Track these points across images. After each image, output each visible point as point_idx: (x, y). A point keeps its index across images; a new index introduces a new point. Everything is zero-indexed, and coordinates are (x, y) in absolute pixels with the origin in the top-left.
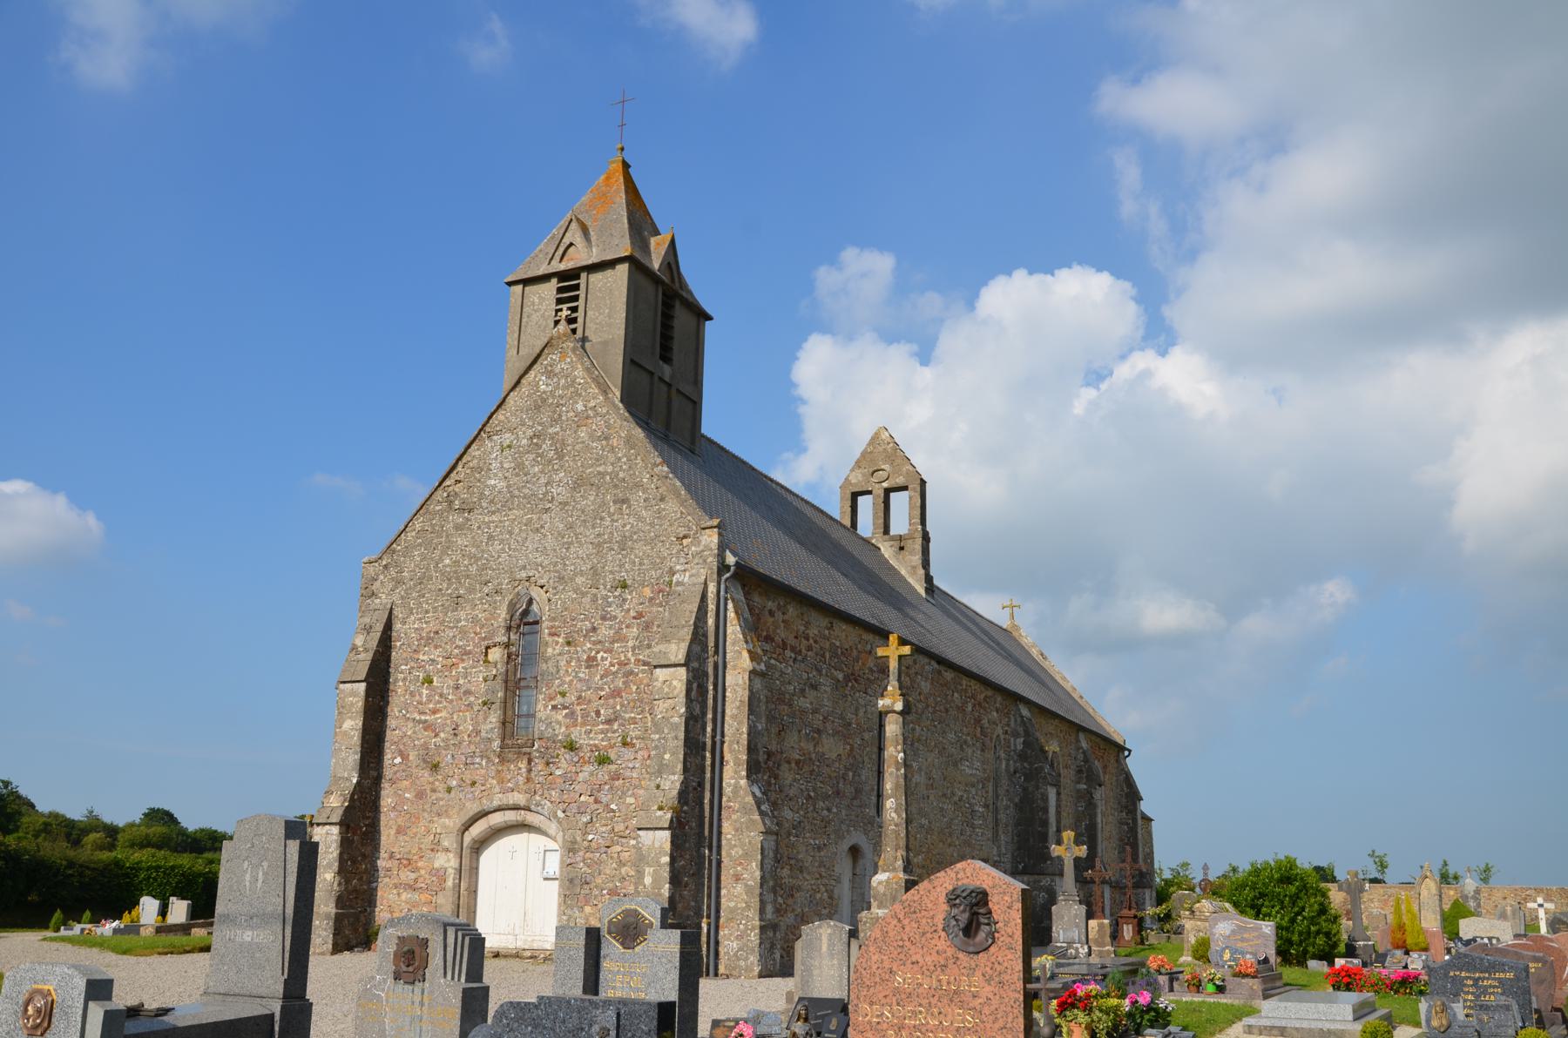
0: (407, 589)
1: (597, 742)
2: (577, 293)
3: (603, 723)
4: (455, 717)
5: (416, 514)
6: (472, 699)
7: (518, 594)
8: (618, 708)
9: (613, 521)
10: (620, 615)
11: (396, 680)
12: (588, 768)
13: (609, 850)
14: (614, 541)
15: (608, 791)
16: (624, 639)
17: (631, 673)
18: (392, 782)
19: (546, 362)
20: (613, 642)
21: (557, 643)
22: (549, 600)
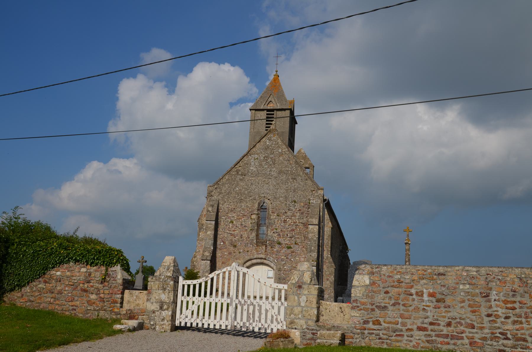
0: (223, 195)
1: (287, 243)
2: (267, 116)
3: (289, 238)
4: (241, 233)
5: (226, 174)
6: (247, 228)
7: (261, 201)
8: (294, 234)
9: (291, 184)
10: (294, 210)
11: (221, 221)
12: (284, 249)
13: (291, 271)
14: (292, 189)
15: (290, 256)
16: (295, 216)
17: (297, 225)
18: (220, 249)
19: (268, 136)
20: (292, 217)
21: (274, 215)
22: (271, 203)
